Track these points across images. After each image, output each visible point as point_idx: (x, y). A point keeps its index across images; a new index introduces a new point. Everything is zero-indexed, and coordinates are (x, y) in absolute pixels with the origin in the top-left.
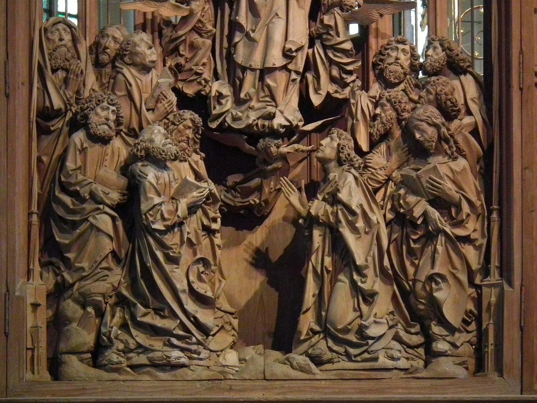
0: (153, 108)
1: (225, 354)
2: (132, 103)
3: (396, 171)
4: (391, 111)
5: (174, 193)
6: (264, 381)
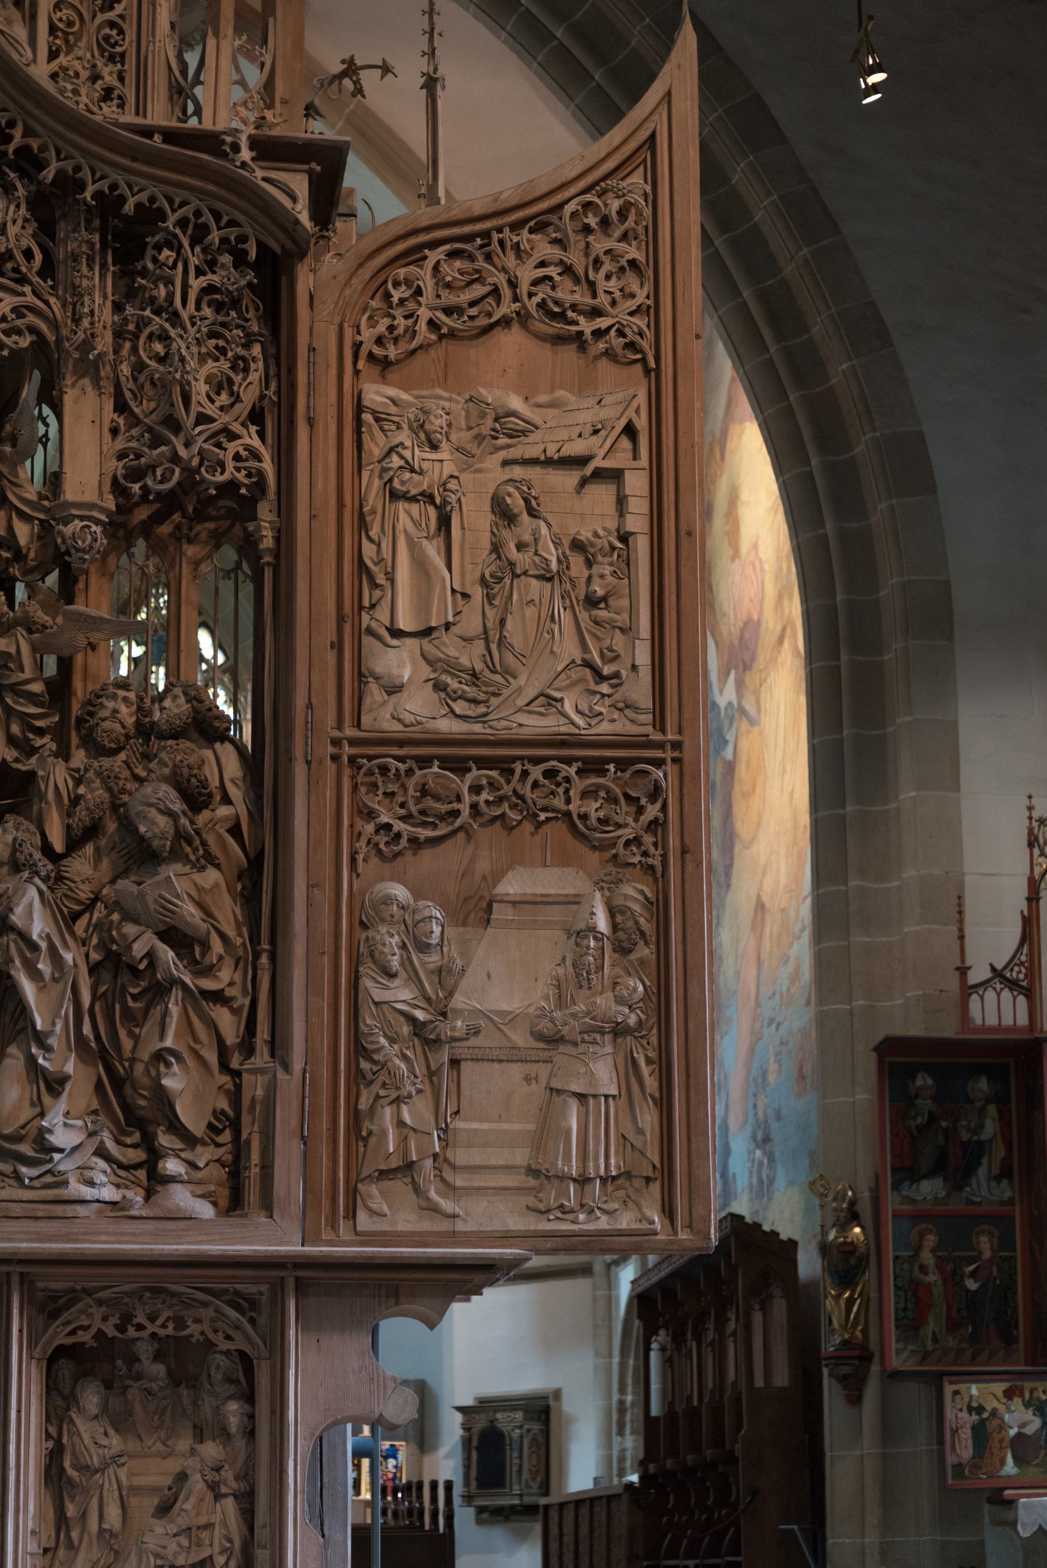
4: (101, 791)
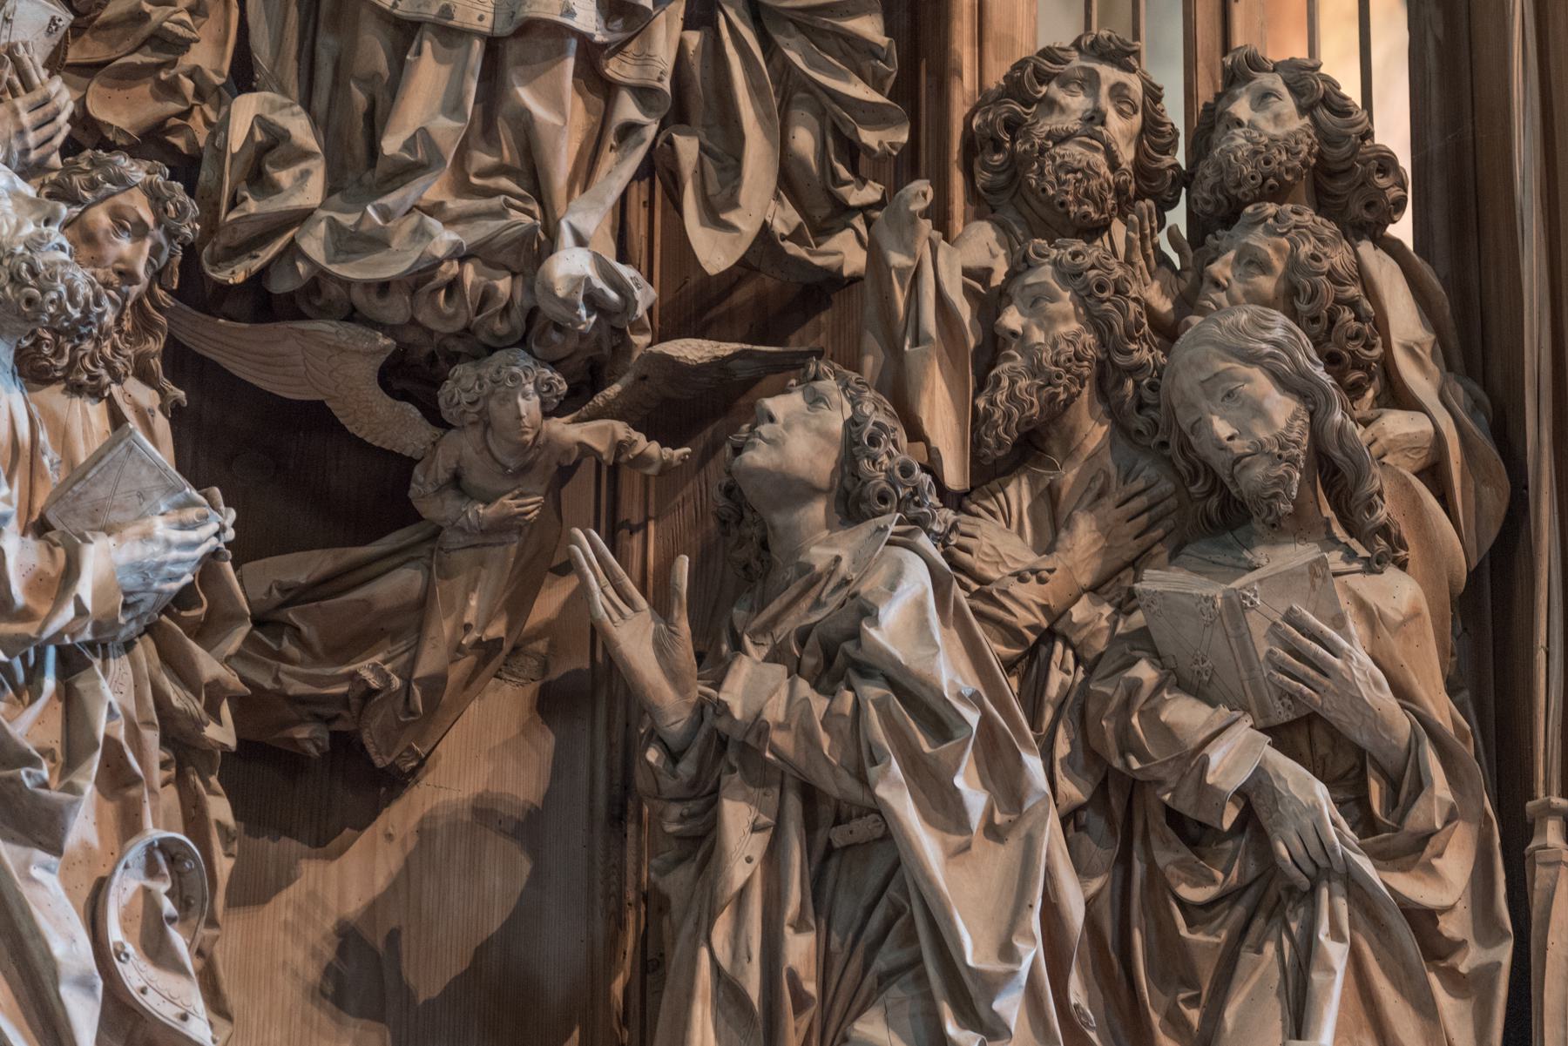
3: (1085, 598)
4: (1075, 326)
5: (57, 497)
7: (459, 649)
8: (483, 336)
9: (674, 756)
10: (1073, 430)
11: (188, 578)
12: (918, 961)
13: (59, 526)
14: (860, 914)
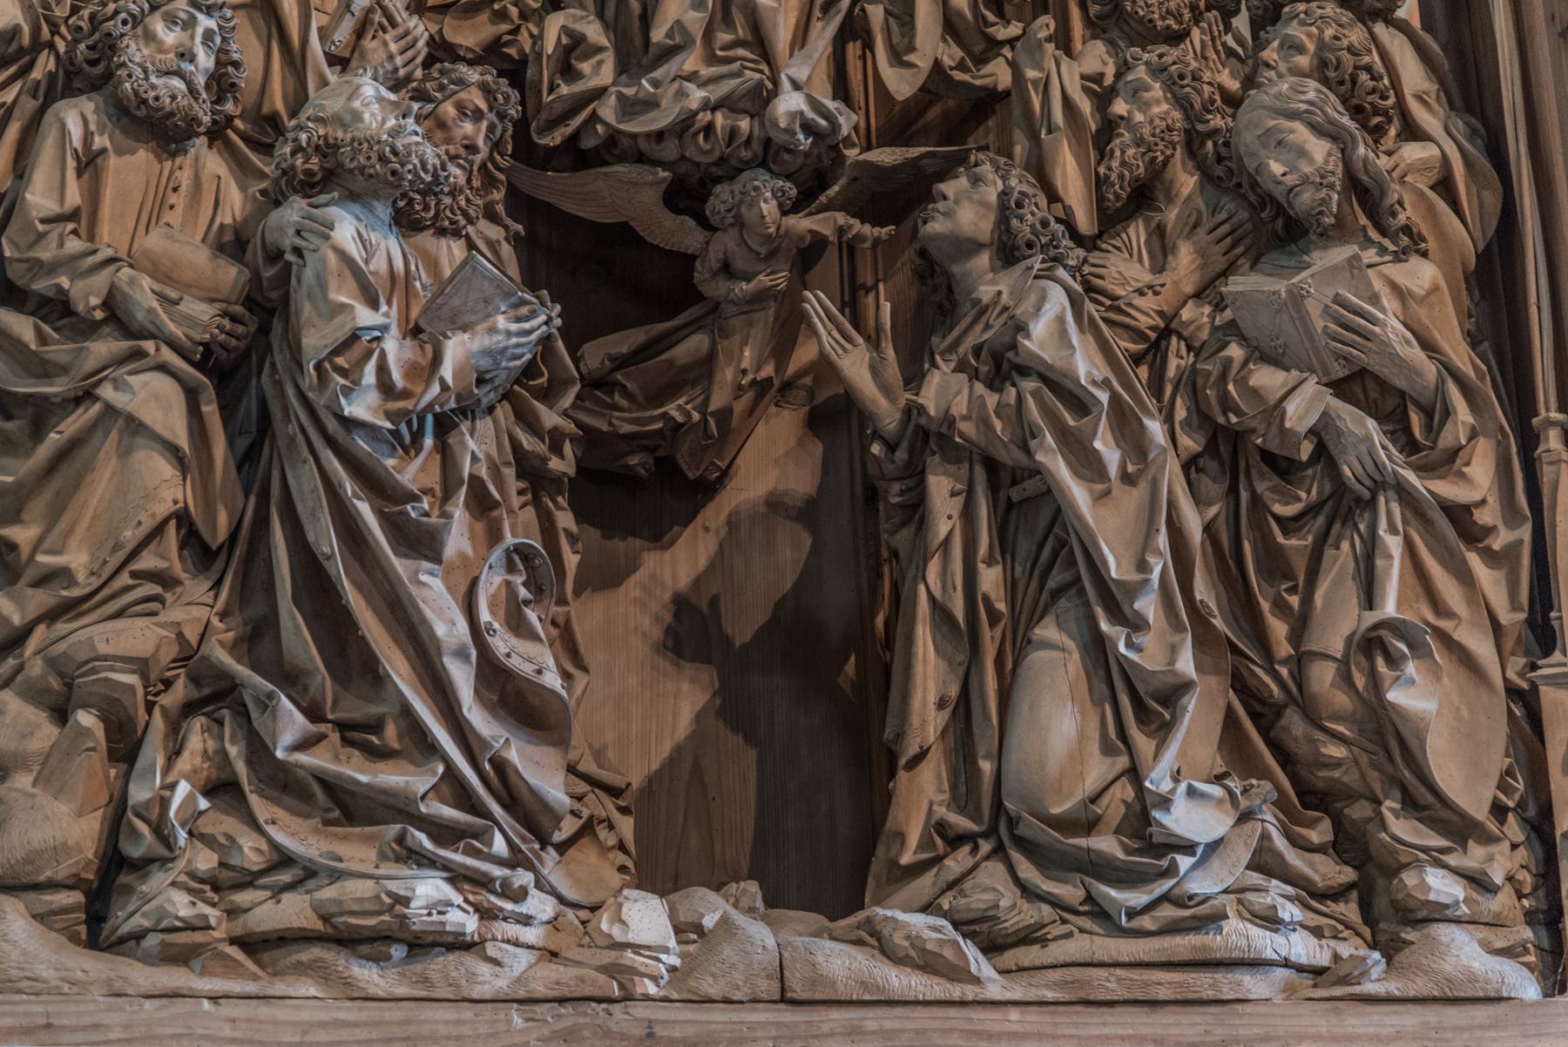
0: (347, 55)
1: (620, 906)
2: (274, 30)
4: (1165, 107)
5: (426, 310)
6: (782, 1006)
7: (739, 389)
8: (734, 163)
9: (891, 447)
10: (1171, 182)
11: (528, 356)
12: (1078, 579)
13: (428, 329)
14: (1034, 548)
